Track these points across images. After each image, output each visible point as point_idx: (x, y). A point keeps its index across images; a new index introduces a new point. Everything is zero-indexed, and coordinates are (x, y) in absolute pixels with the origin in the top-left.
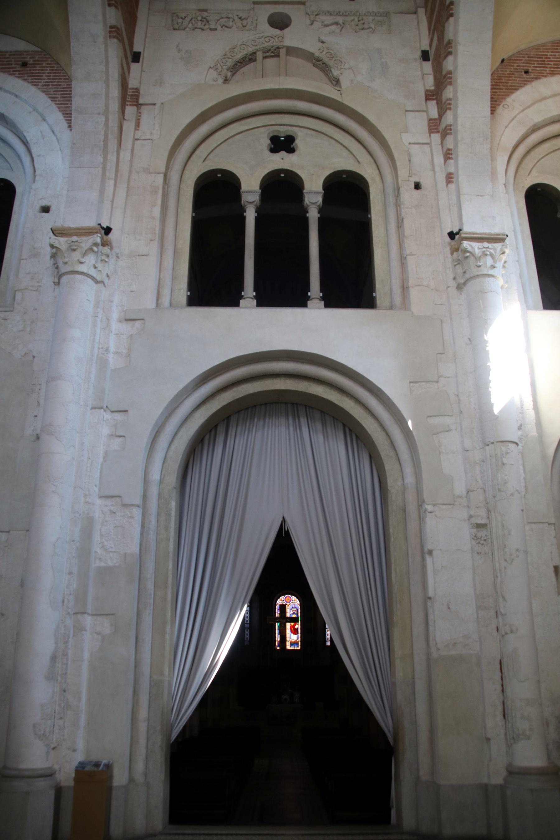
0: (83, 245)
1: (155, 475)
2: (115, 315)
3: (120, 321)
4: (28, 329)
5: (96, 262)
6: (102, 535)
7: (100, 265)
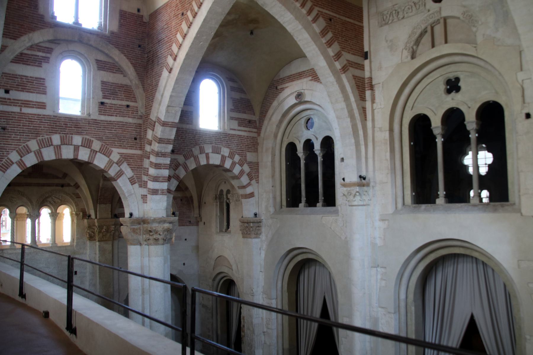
0: (352, 192)
1: (403, 296)
2: (377, 217)
3: (380, 220)
4: (345, 225)
5: (361, 198)
6: (381, 324)
7: (364, 197)
